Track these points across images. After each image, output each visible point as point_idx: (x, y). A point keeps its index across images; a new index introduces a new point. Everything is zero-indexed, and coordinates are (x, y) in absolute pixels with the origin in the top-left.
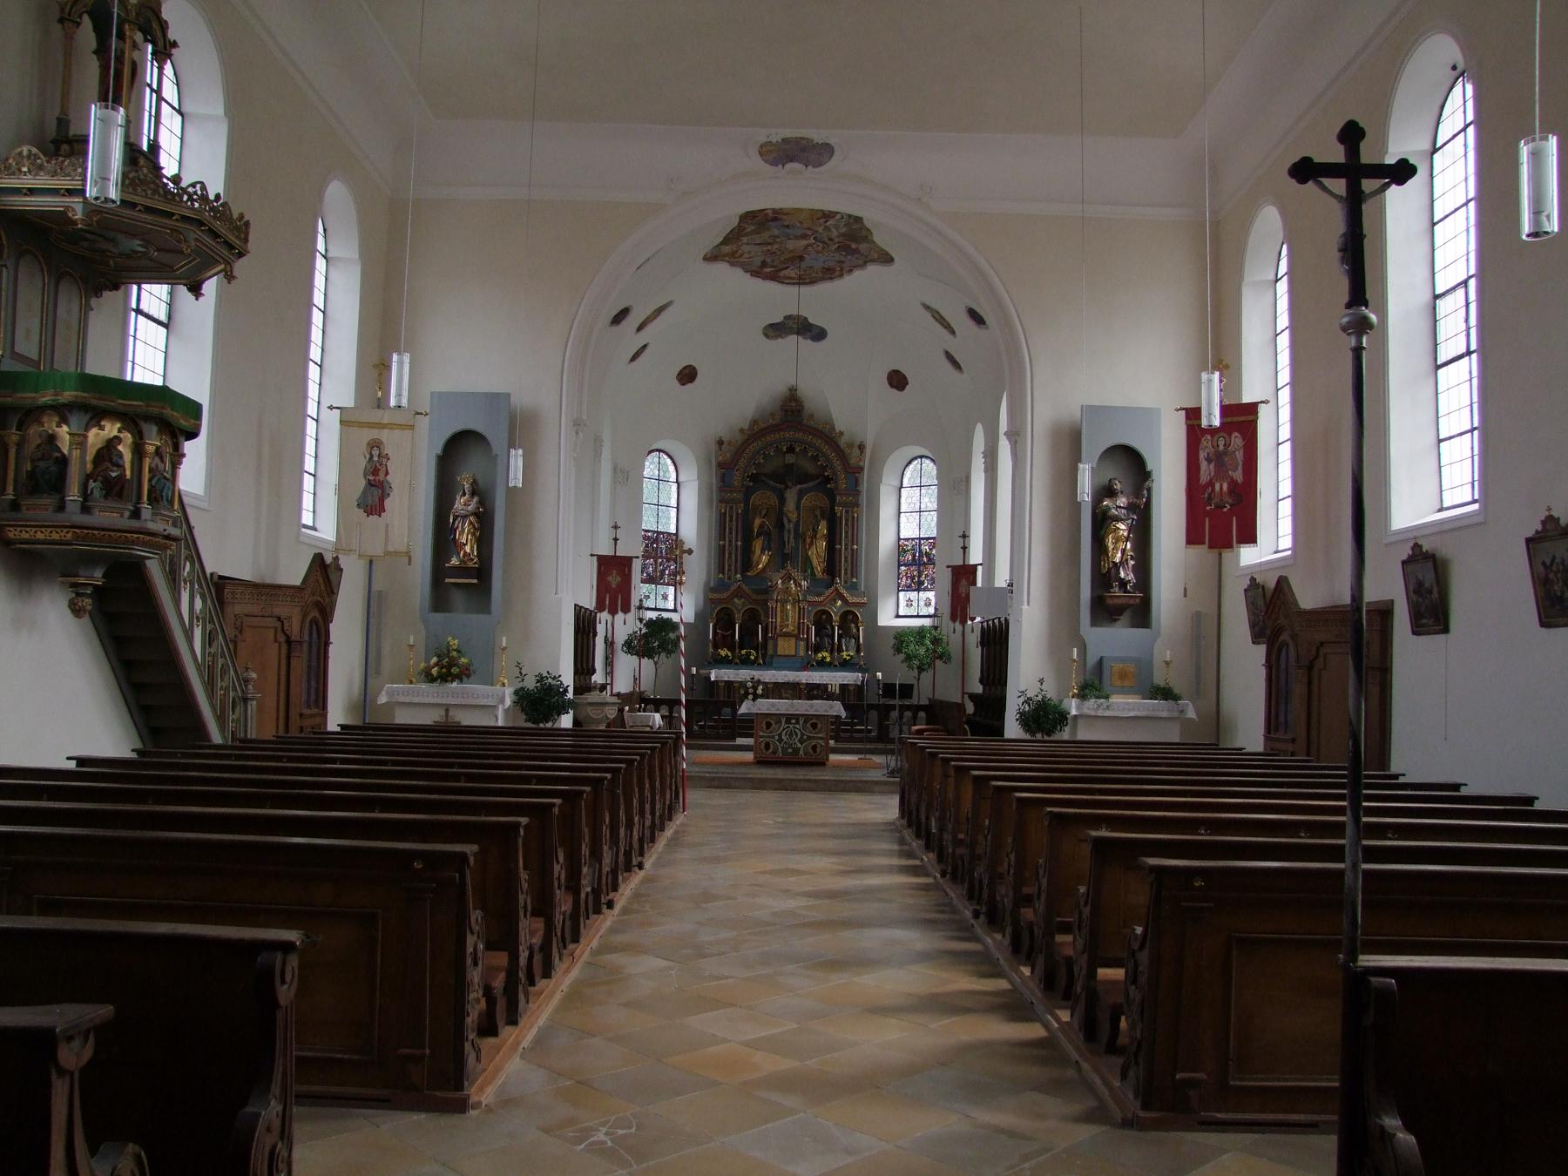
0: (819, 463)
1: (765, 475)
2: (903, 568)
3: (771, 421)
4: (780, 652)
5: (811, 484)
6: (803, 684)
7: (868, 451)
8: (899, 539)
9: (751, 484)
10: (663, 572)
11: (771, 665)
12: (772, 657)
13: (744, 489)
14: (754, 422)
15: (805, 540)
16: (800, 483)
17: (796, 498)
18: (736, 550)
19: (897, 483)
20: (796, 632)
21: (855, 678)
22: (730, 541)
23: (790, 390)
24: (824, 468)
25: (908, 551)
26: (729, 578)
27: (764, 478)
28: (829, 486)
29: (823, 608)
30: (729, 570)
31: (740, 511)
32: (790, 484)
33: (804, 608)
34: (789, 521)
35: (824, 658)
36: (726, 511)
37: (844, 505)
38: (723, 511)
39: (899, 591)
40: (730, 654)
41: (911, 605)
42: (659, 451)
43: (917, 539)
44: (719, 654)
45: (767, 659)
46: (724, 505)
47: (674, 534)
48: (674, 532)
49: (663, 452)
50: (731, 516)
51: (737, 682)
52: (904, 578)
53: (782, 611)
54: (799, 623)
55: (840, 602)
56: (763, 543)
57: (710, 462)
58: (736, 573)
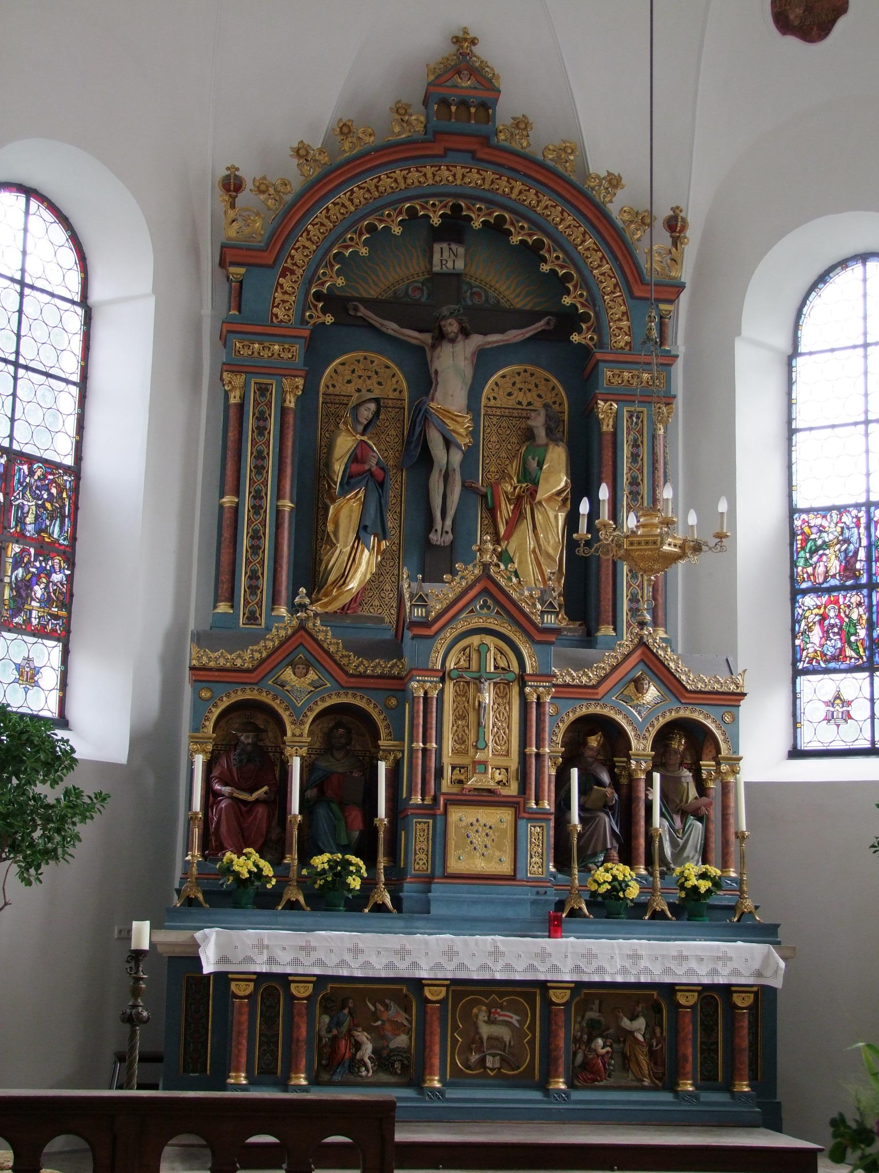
0: (545, 268)
1: (364, 301)
2: (809, 601)
3: (397, 129)
4: (457, 864)
5: (514, 335)
6: (560, 985)
7: (693, 234)
8: (792, 511)
9: (329, 319)
10: (23, 590)
11: (425, 909)
12: (428, 880)
13: (306, 333)
14: (345, 129)
15: (492, 512)
16: (485, 334)
17: (469, 373)
18: (278, 525)
19: (783, 343)
20: (513, 789)
21: (756, 965)
22: (258, 496)
23: (454, 43)
24: (560, 284)
25: (826, 545)
26: (252, 618)
27: (363, 311)
28: (575, 338)
29: (598, 710)
30: (253, 589)
31: (291, 402)
32: (452, 327)
33: (540, 704)
34: (448, 443)
35: (618, 885)
36: (243, 398)
37: (623, 397)
38: (234, 400)
39: (797, 673)
40: (268, 870)
41: (848, 716)
42: (29, 192)
43: (857, 506)
44: (228, 870)
45: (409, 889)
46: (239, 380)
47: (67, 469)
48: (69, 461)
49: (42, 199)
50: (262, 417)
51: (303, 979)
52: (816, 635)
53: (460, 716)
54: (524, 757)
55: (652, 693)
56: (364, 504)
57: (195, 250)
58: (275, 600)
